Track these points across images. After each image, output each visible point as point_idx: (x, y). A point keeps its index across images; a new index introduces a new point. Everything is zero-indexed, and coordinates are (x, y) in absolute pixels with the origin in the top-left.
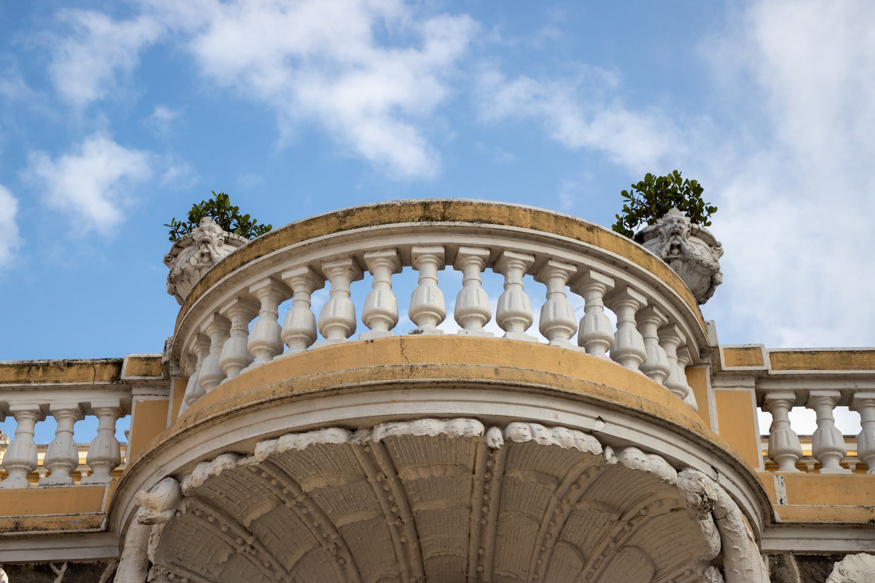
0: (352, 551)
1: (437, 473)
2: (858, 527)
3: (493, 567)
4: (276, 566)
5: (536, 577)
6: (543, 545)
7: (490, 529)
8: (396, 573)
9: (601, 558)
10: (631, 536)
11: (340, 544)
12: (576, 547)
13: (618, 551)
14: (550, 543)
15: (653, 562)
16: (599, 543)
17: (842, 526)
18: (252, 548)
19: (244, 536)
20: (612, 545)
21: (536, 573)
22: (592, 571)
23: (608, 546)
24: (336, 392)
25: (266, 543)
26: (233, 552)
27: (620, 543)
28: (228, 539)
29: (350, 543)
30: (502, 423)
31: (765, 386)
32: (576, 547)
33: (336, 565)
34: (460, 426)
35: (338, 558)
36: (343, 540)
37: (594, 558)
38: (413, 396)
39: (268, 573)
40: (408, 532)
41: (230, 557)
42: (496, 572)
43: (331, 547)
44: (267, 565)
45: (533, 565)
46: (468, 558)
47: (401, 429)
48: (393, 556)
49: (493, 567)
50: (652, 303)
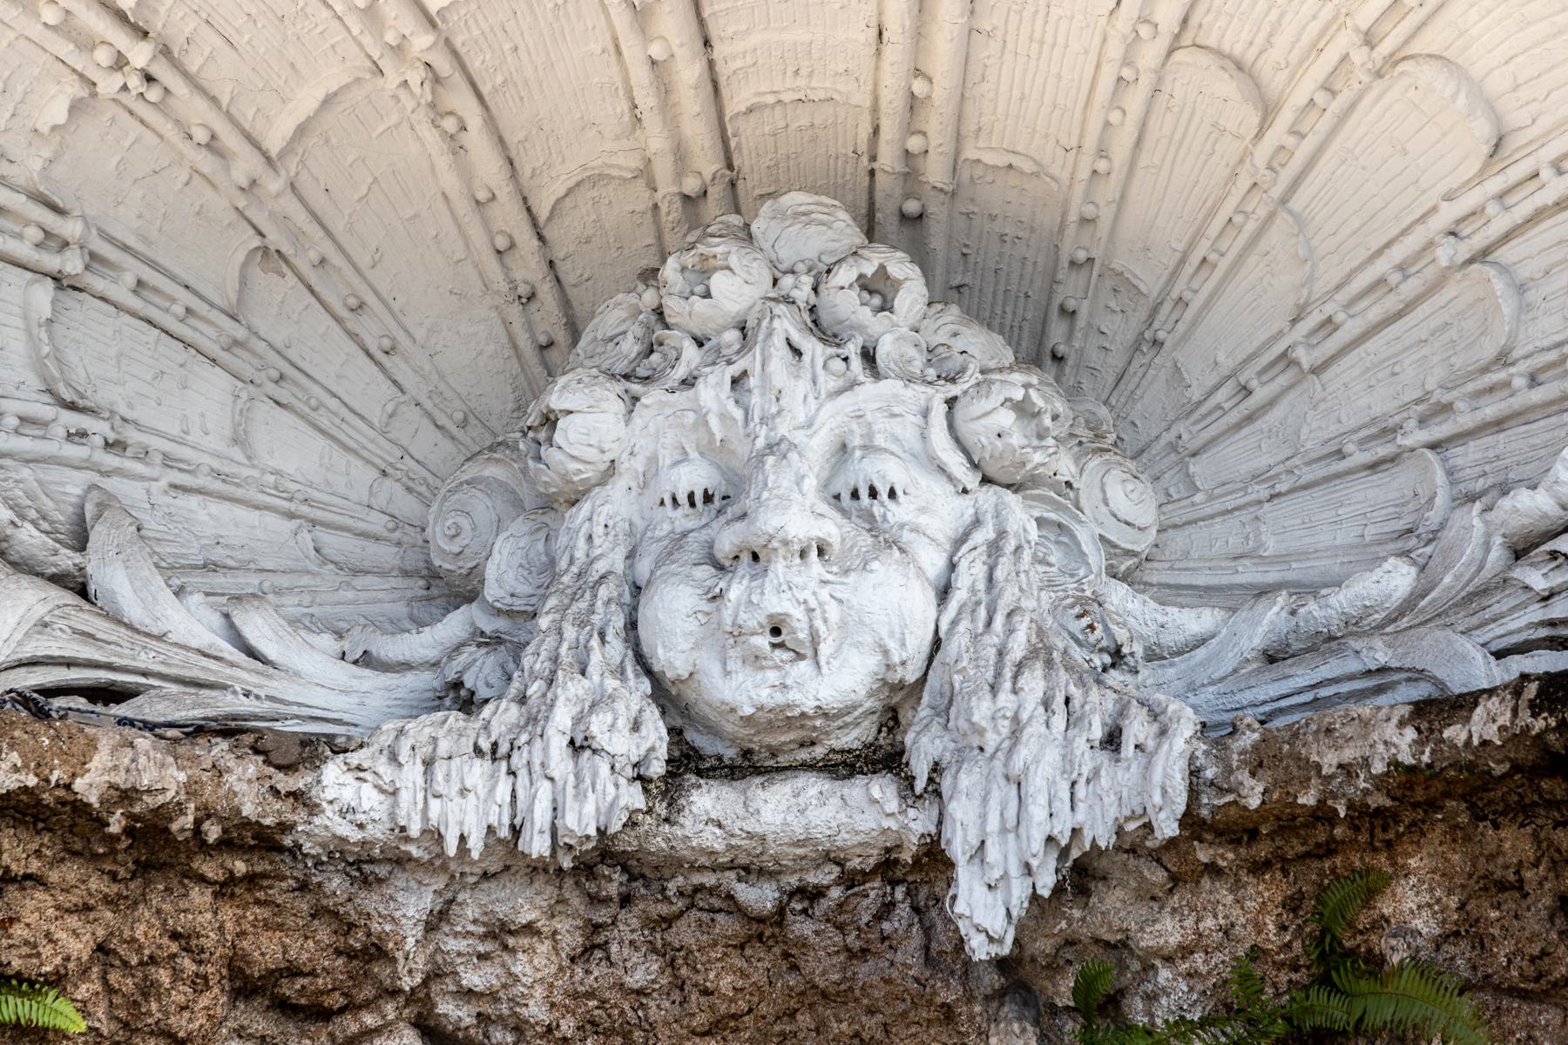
0: (485, 90)
3: (959, 138)
4: (230, 139)
5: (1102, 166)
6: (1127, 61)
8: (634, 162)
9: (1321, 98)
10: (1423, 25)
11: (444, 65)
13: (1379, 75)
14: (1150, 55)
15: (1490, 107)
16: (1316, 49)
18: (149, 79)
19: (122, 39)
20: (1359, 56)
21: (1102, 153)
22: (1290, 141)
23: (1345, 58)
25: (193, 64)
26: (84, 93)
27: (1385, 48)
28: (65, 49)
29: (475, 64)
33: (431, 137)
35: (436, 111)
36: (455, 54)
37: (1299, 98)
39: (205, 162)
41: (75, 108)
42: (970, 153)
43: (416, 76)
44: (201, 135)
45: (1094, 127)
46: (875, 109)
48: (624, 106)
49: (959, 138)
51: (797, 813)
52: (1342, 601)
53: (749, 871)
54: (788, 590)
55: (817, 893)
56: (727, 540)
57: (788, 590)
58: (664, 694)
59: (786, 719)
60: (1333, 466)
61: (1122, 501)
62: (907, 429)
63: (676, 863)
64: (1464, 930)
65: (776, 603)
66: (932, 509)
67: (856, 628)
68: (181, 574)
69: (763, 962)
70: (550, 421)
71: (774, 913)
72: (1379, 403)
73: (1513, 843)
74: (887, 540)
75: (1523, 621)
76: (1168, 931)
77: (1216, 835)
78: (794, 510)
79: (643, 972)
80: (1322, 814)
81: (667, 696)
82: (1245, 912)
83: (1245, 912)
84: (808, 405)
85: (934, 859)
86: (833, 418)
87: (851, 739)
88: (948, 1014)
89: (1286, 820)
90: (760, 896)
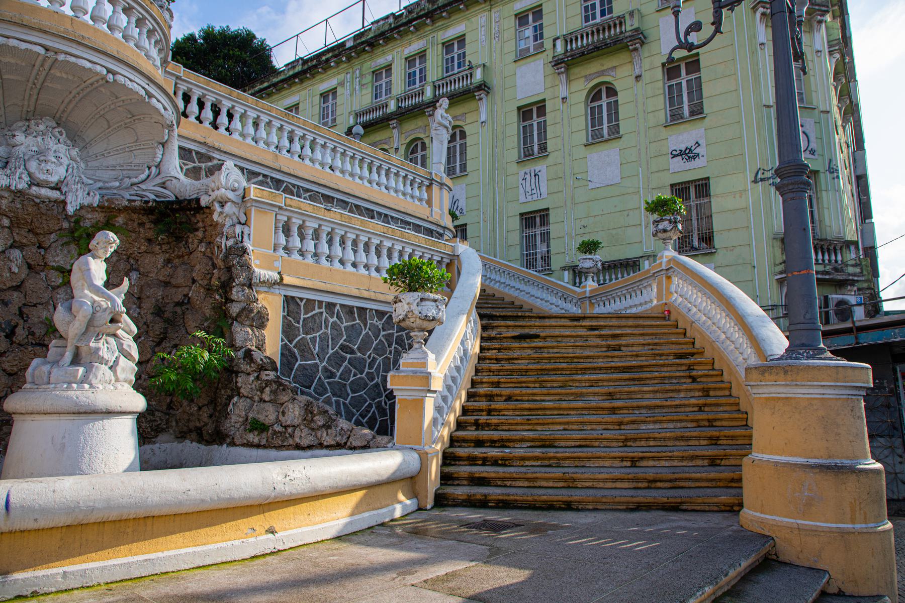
1: (70, 77)
2: (200, 143)
7: (74, 103)
12: (108, 121)
14: (97, 116)
17: (195, 141)
24: (45, 32)
30: (114, 73)
31: (178, 81)
32: (108, 121)
34: (99, 68)
38: (81, 48)
40: (35, 91)
47: (73, 59)
50: (161, 40)
51: (45, 192)
52: (111, 184)
53: (37, 197)
54: (50, 166)
55: (44, 202)
56: (42, 158)
57: (50, 166)
58: (30, 174)
59: (46, 181)
60: (114, 168)
62: (64, 151)
63: (28, 194)
64: (126, 224)
65: (48, 168)
66: (65, 161)
67: (58, 173)
69: (35, 208)
70: (14, 136)
71: (39, 204)
72: (114, 163)
73: (135, 216)
74: (61, 164)
75: (133, 192)
76: (90, 216)
79: (19, 206)
80: (114, 208)
81: (30, 174)
84: (52, 145)
85: (64, 203)
86: (55, 147)
87: (52, 185)
88: (59, 219)
89: (109, 208)
90: (38, 201)
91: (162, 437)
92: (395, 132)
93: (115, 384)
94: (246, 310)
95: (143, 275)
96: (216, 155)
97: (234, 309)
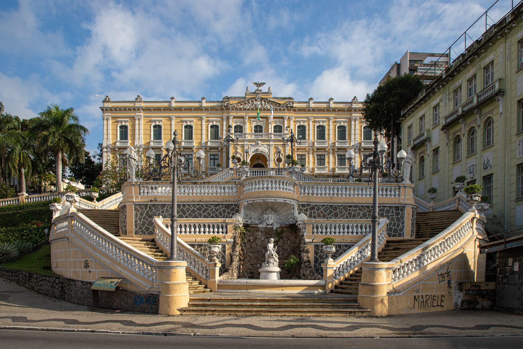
61: (278, 217)
66: (273, 218)
67: (271, 221)
68: (253, 218)
71: (269, 229)
77: (280, 227)
78: (270, 219)
82: (281, 229)
83: (281, 229)
84: (270, 215)
85: (273, 228)
91: (294, 277)
92: (462, 125)
93: (274, 267)
94: (303, 250)
95: (291, 241)
96: (311, 204)
97: (301, 249)
